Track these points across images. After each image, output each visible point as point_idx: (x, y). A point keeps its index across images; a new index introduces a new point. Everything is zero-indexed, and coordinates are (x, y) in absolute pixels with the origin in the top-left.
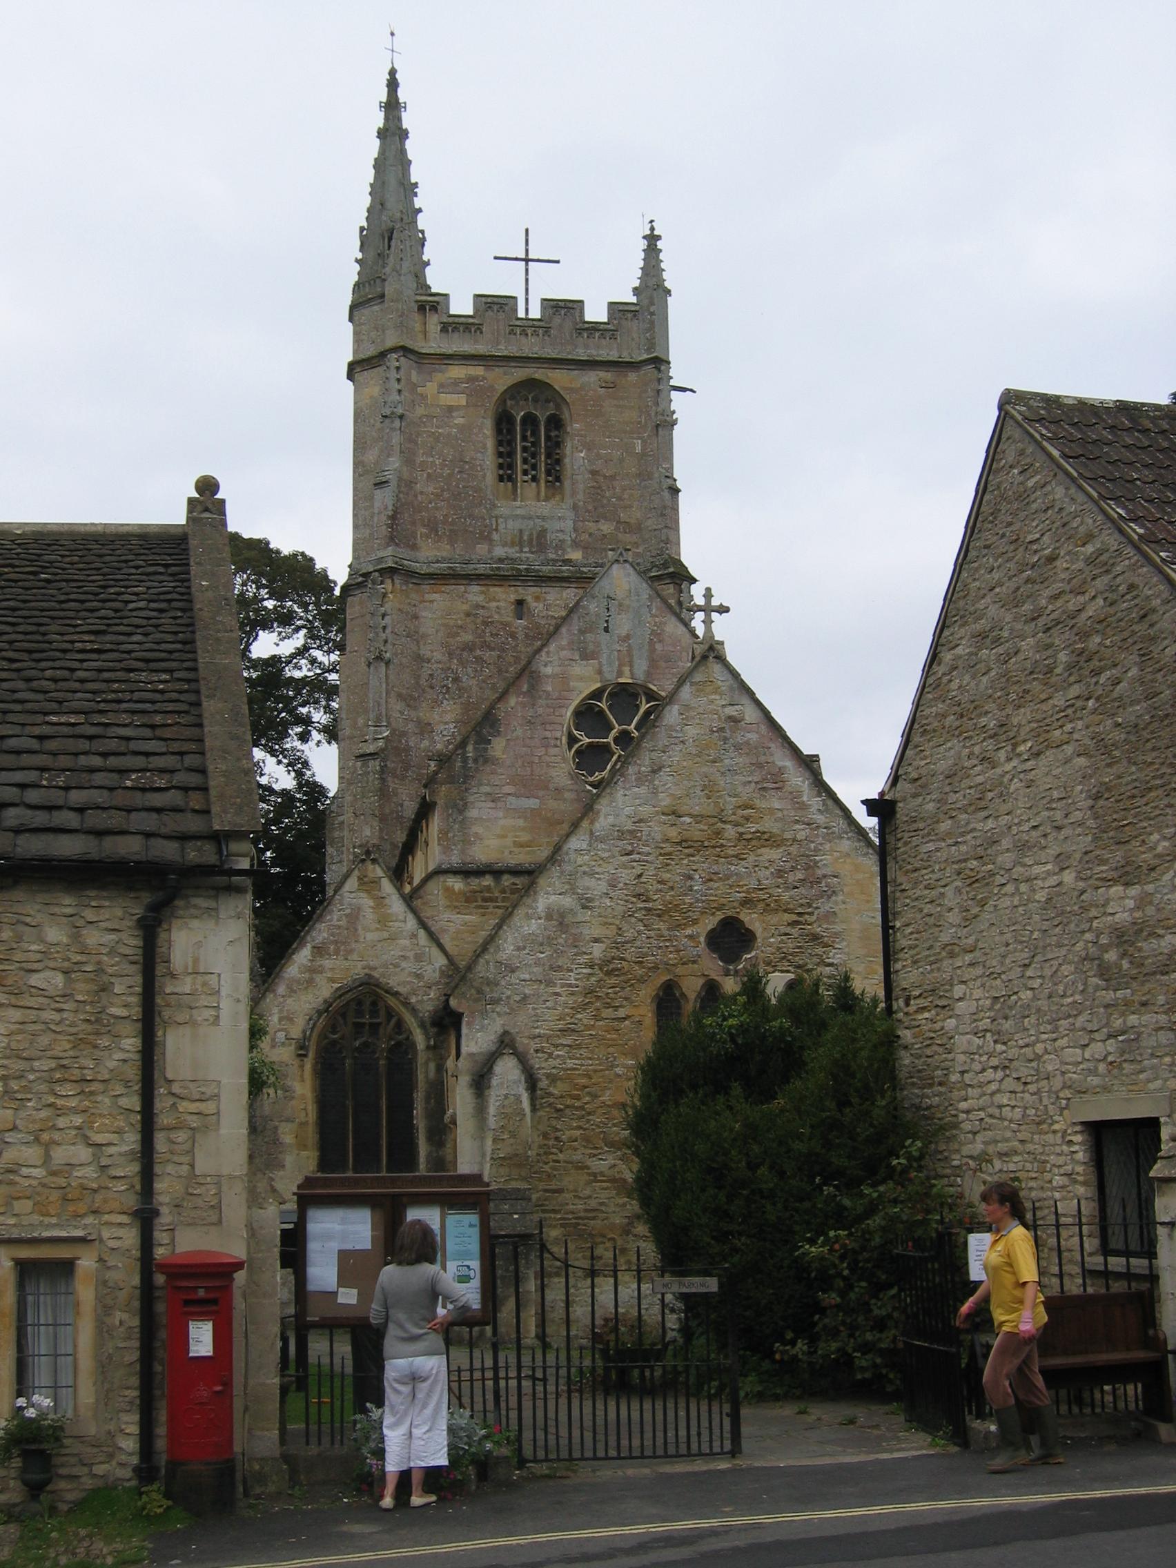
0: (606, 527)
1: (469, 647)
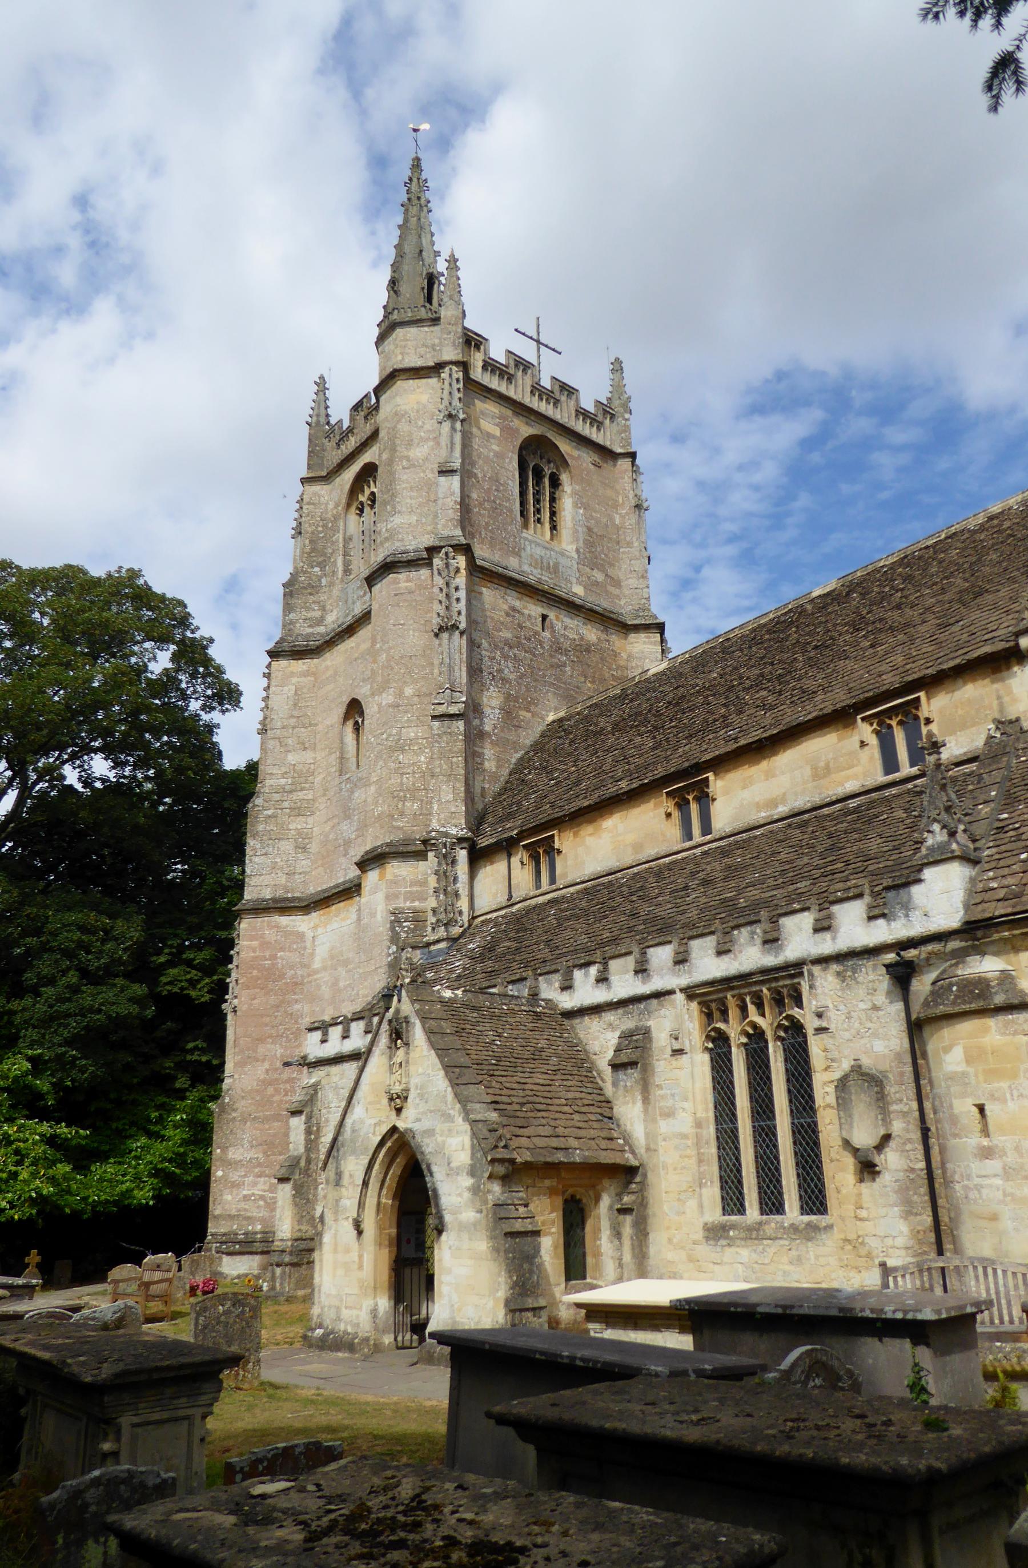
0: (599, 577)
1: (507, 643)
